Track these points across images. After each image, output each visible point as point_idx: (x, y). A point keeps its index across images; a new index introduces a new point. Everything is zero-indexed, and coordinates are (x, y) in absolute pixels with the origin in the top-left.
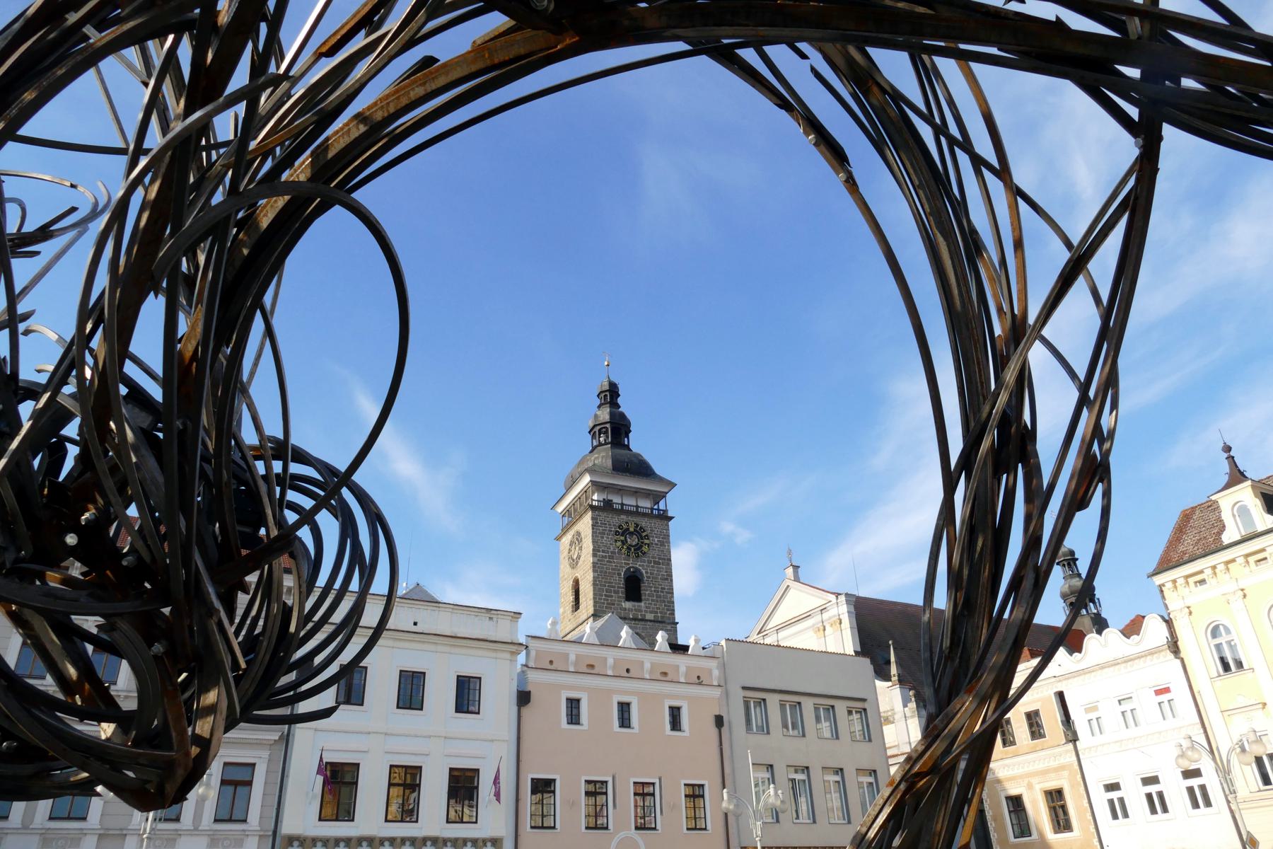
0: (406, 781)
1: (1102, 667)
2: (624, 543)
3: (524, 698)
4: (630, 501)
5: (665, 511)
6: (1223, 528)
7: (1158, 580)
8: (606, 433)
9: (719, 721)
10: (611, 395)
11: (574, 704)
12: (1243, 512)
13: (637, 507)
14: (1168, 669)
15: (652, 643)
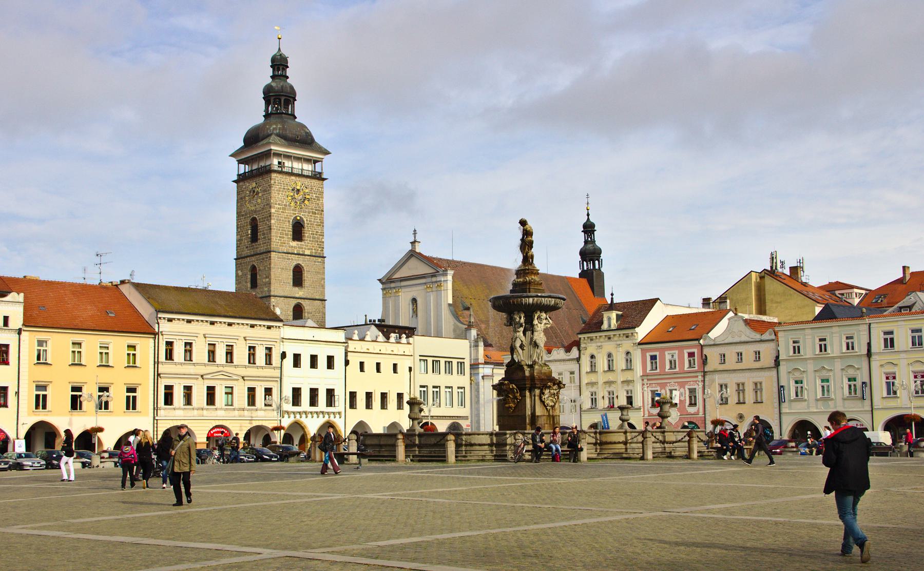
0: (314, 393)
1: (556, 361)
2: (293, 198)
3: (347, 363)
4: (297, 166)
5: (320, 173)
6: (602, 323)
7: (580, 336)
8: (280, 104)
9: (410, 369)
10: (279, 64)
11: (362, 364)
12: (609, 319)
13: (302, 170)
14: (574, 366)
15: (388, 338)
